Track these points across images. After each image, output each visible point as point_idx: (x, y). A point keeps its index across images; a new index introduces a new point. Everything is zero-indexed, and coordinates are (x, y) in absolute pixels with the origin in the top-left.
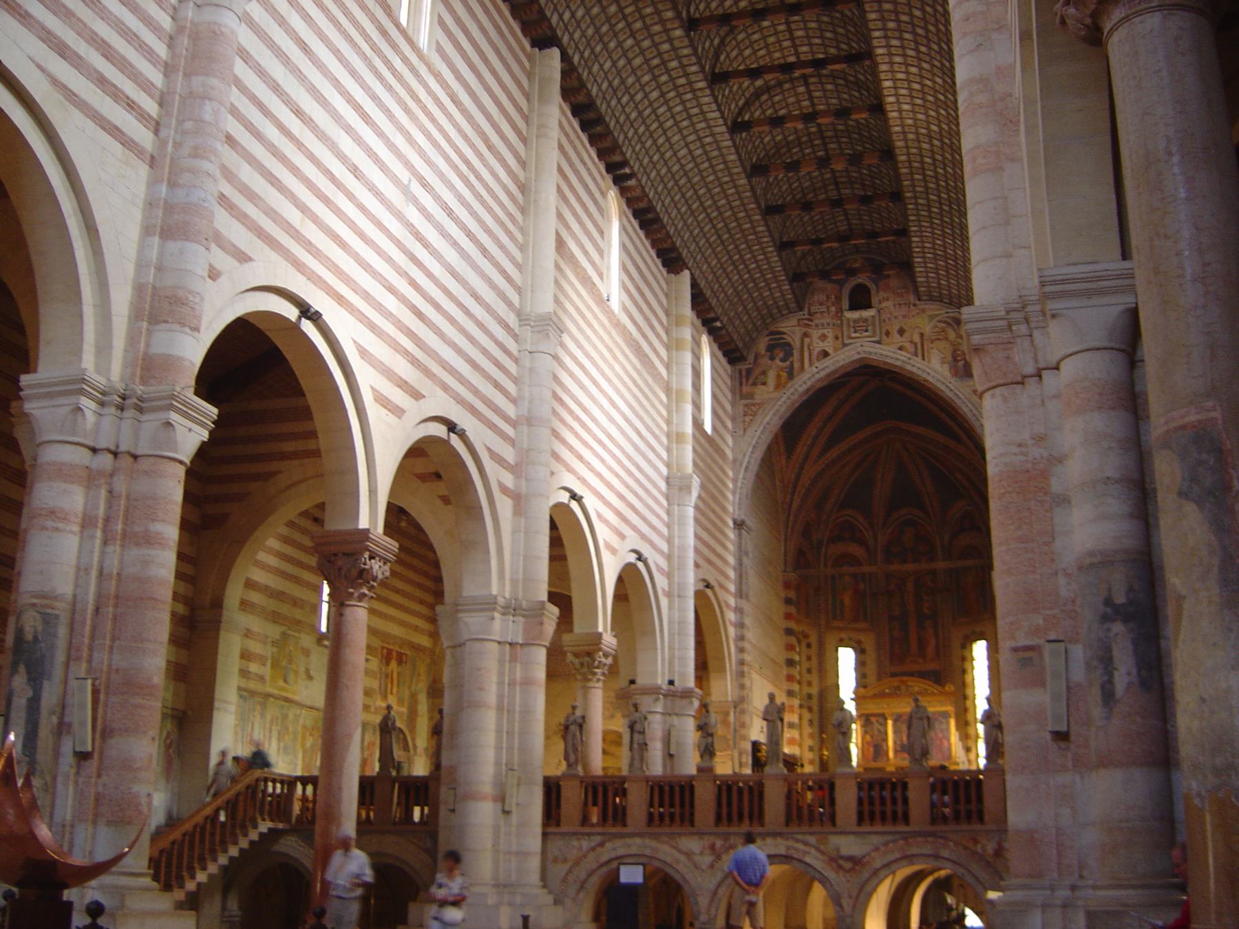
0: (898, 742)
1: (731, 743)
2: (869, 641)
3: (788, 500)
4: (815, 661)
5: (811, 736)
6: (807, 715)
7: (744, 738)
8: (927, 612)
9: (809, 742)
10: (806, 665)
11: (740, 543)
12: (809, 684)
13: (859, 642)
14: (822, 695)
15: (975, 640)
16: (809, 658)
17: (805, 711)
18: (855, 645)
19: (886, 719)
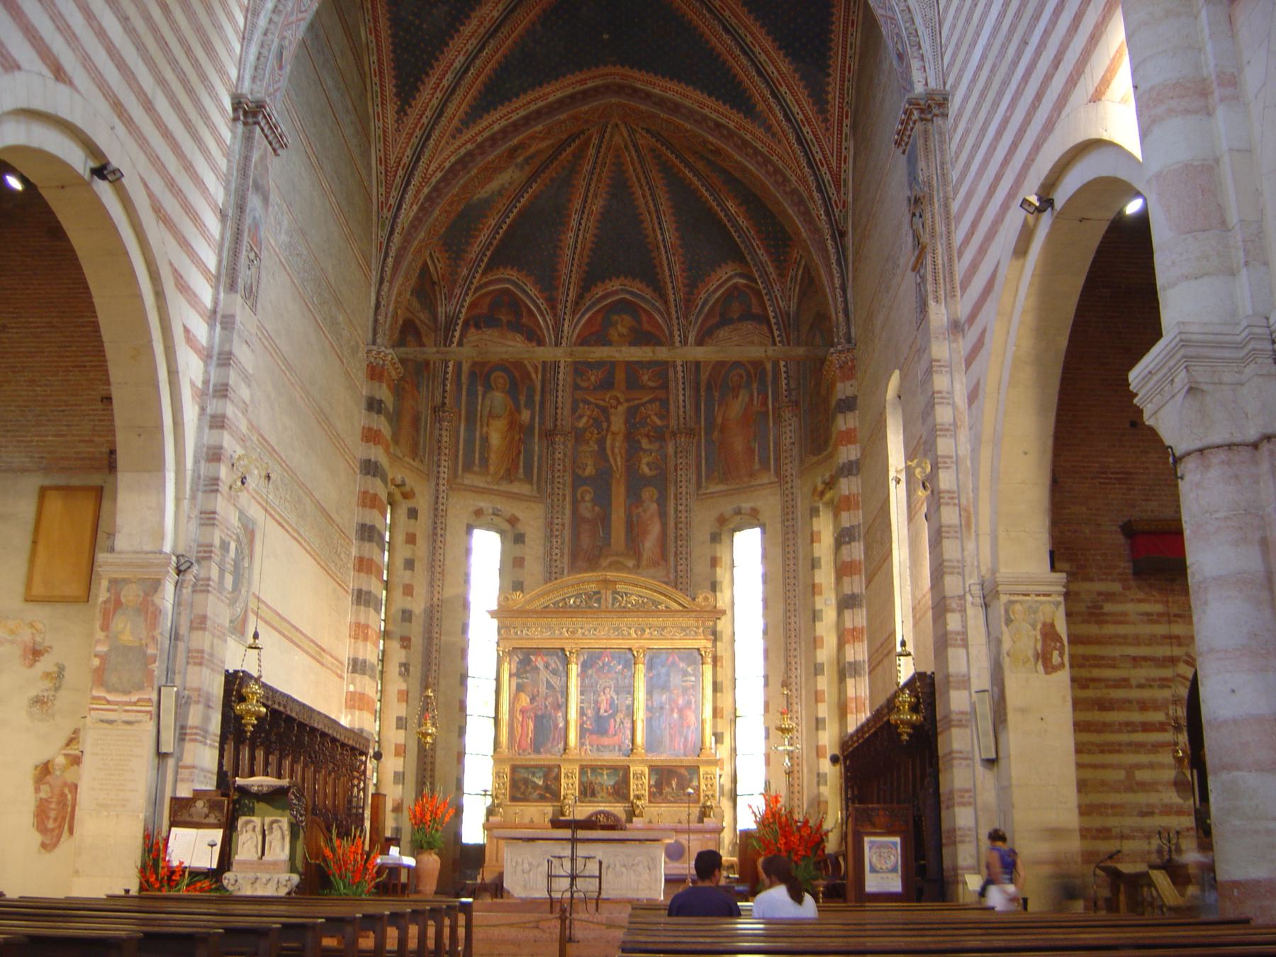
0: (590, 713)
1: (158, 668)
2: (532, 519)
3: (392, 201)
4: (422, 547)
5: (404, 696)
6: (398, 654)
7: (198, 658)
8: (646, 470)
9: (397, 709)
10: (403, 552)
11: (247, 158)
12: (408, 590)
13: (513, 521)
14: (432, 614)
15: (739, 528)
16: (411, 539)
17: (395, 645)
18: (507, 526)
19: (566, 662)
